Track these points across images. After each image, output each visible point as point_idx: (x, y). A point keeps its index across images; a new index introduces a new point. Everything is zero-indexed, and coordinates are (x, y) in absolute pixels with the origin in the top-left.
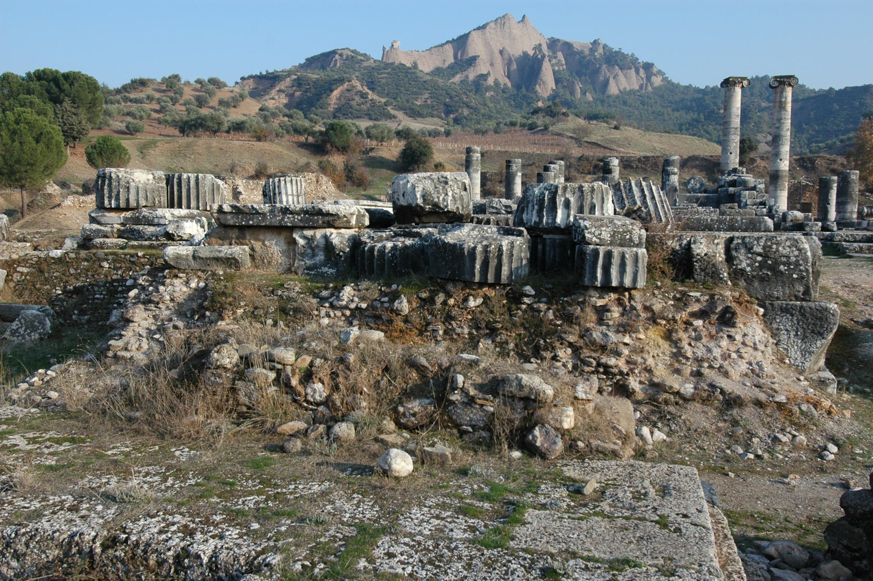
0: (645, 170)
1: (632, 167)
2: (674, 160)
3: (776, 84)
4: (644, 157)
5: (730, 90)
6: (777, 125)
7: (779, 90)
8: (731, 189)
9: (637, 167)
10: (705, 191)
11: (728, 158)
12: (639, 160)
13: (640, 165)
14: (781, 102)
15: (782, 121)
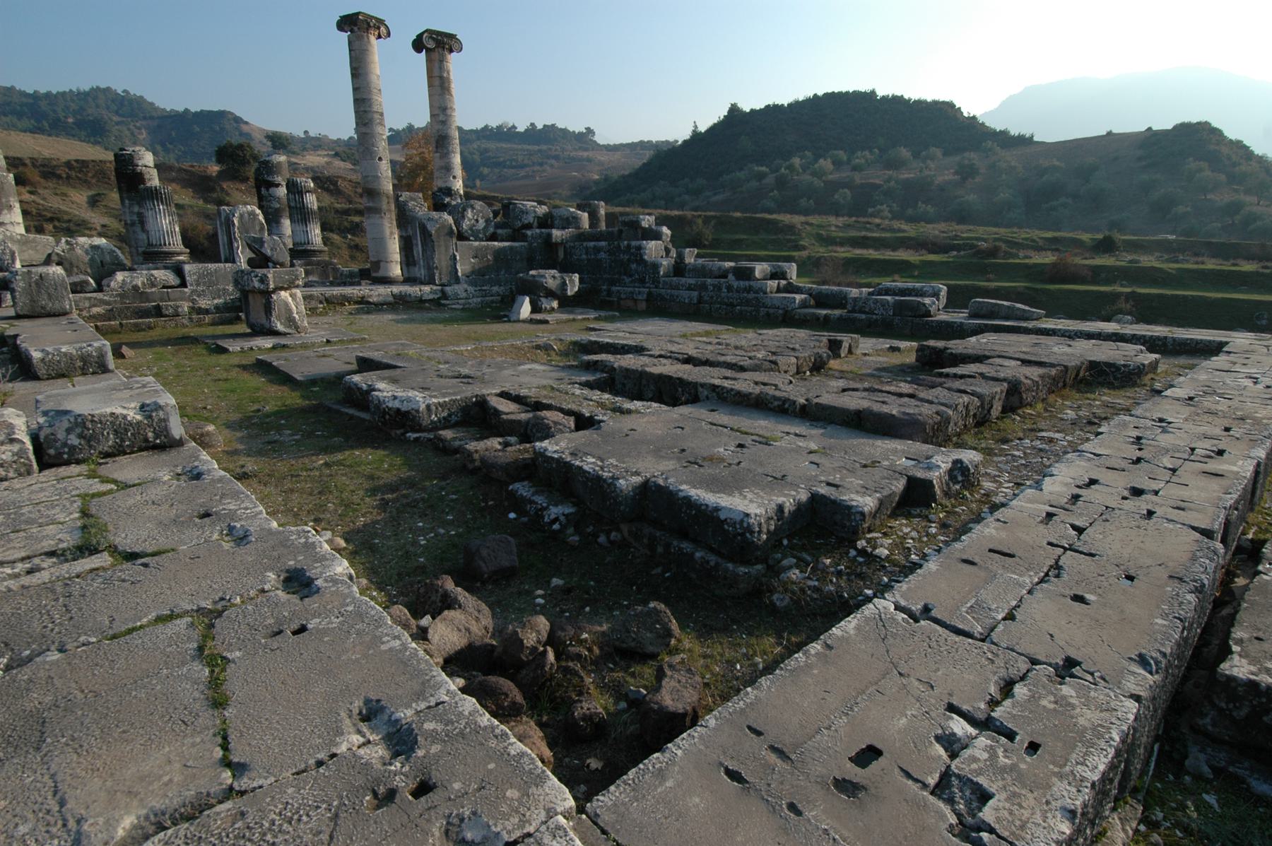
0: (86, 181)
1: (59, 177)
2: (279, 163)
3: (431, 45)
4: (77, 161)
5: (360, 38)
6: (441, 118)
7: (435, 55)
8: (557, 234)
9: (68, 177)
10: (493, 237)
11: (376, 168)
12: (68, 164)
13: (73, 174)
14: (441, 77)
15: (449, 112)
